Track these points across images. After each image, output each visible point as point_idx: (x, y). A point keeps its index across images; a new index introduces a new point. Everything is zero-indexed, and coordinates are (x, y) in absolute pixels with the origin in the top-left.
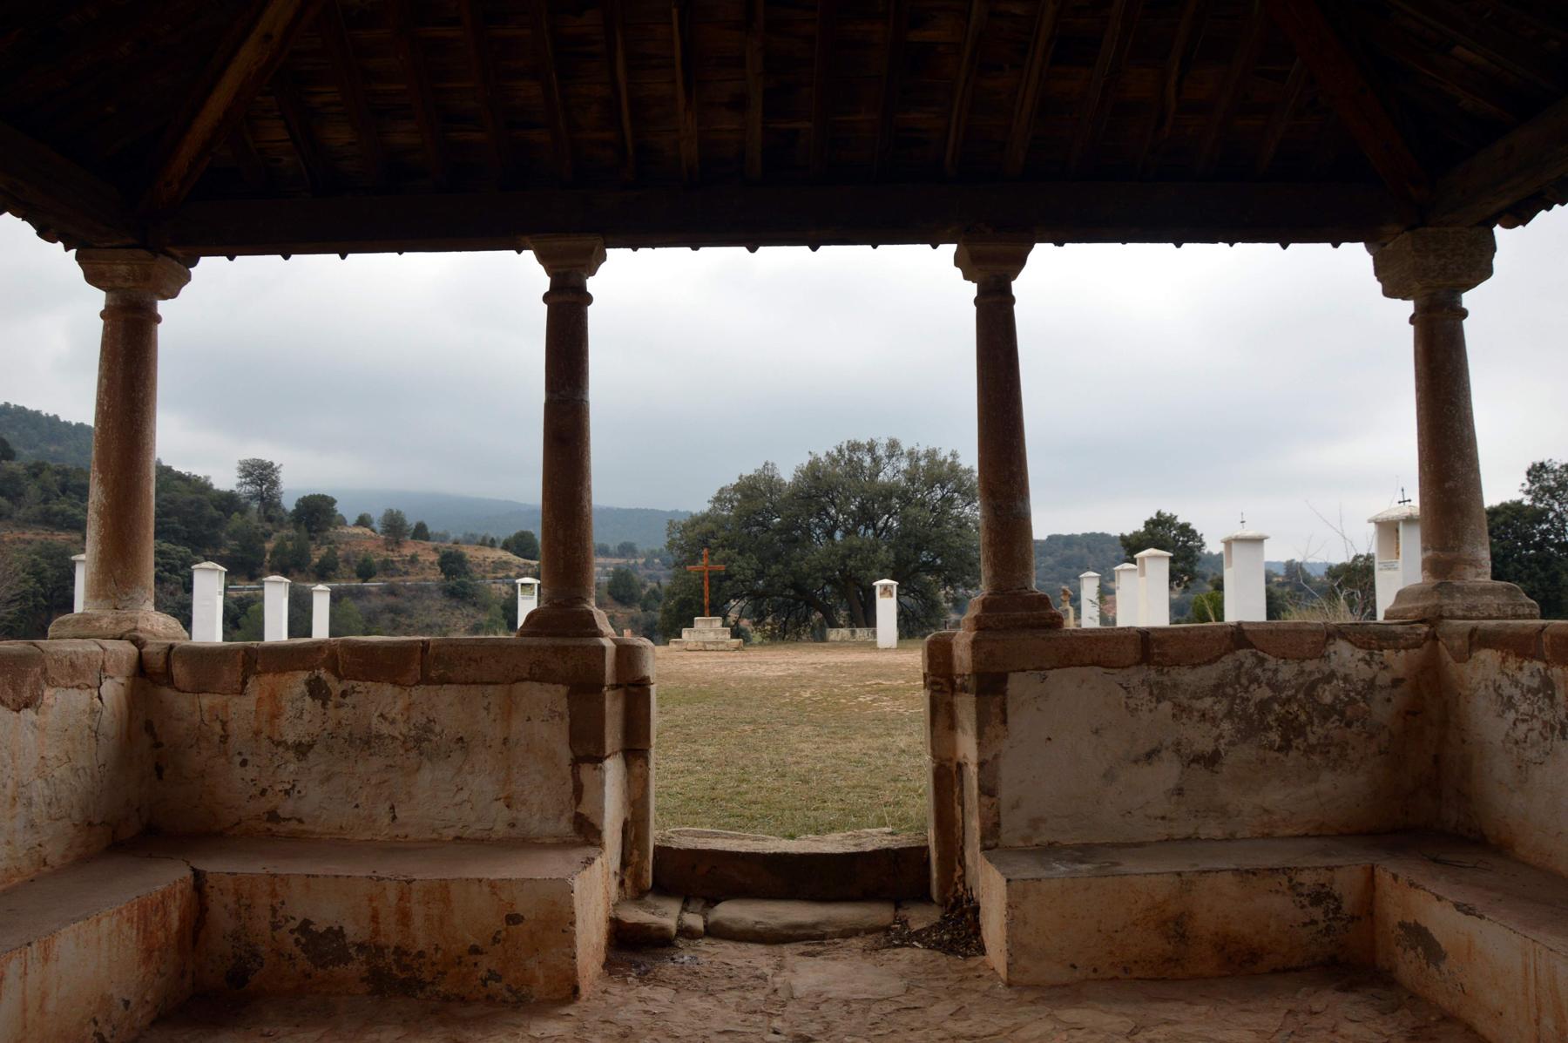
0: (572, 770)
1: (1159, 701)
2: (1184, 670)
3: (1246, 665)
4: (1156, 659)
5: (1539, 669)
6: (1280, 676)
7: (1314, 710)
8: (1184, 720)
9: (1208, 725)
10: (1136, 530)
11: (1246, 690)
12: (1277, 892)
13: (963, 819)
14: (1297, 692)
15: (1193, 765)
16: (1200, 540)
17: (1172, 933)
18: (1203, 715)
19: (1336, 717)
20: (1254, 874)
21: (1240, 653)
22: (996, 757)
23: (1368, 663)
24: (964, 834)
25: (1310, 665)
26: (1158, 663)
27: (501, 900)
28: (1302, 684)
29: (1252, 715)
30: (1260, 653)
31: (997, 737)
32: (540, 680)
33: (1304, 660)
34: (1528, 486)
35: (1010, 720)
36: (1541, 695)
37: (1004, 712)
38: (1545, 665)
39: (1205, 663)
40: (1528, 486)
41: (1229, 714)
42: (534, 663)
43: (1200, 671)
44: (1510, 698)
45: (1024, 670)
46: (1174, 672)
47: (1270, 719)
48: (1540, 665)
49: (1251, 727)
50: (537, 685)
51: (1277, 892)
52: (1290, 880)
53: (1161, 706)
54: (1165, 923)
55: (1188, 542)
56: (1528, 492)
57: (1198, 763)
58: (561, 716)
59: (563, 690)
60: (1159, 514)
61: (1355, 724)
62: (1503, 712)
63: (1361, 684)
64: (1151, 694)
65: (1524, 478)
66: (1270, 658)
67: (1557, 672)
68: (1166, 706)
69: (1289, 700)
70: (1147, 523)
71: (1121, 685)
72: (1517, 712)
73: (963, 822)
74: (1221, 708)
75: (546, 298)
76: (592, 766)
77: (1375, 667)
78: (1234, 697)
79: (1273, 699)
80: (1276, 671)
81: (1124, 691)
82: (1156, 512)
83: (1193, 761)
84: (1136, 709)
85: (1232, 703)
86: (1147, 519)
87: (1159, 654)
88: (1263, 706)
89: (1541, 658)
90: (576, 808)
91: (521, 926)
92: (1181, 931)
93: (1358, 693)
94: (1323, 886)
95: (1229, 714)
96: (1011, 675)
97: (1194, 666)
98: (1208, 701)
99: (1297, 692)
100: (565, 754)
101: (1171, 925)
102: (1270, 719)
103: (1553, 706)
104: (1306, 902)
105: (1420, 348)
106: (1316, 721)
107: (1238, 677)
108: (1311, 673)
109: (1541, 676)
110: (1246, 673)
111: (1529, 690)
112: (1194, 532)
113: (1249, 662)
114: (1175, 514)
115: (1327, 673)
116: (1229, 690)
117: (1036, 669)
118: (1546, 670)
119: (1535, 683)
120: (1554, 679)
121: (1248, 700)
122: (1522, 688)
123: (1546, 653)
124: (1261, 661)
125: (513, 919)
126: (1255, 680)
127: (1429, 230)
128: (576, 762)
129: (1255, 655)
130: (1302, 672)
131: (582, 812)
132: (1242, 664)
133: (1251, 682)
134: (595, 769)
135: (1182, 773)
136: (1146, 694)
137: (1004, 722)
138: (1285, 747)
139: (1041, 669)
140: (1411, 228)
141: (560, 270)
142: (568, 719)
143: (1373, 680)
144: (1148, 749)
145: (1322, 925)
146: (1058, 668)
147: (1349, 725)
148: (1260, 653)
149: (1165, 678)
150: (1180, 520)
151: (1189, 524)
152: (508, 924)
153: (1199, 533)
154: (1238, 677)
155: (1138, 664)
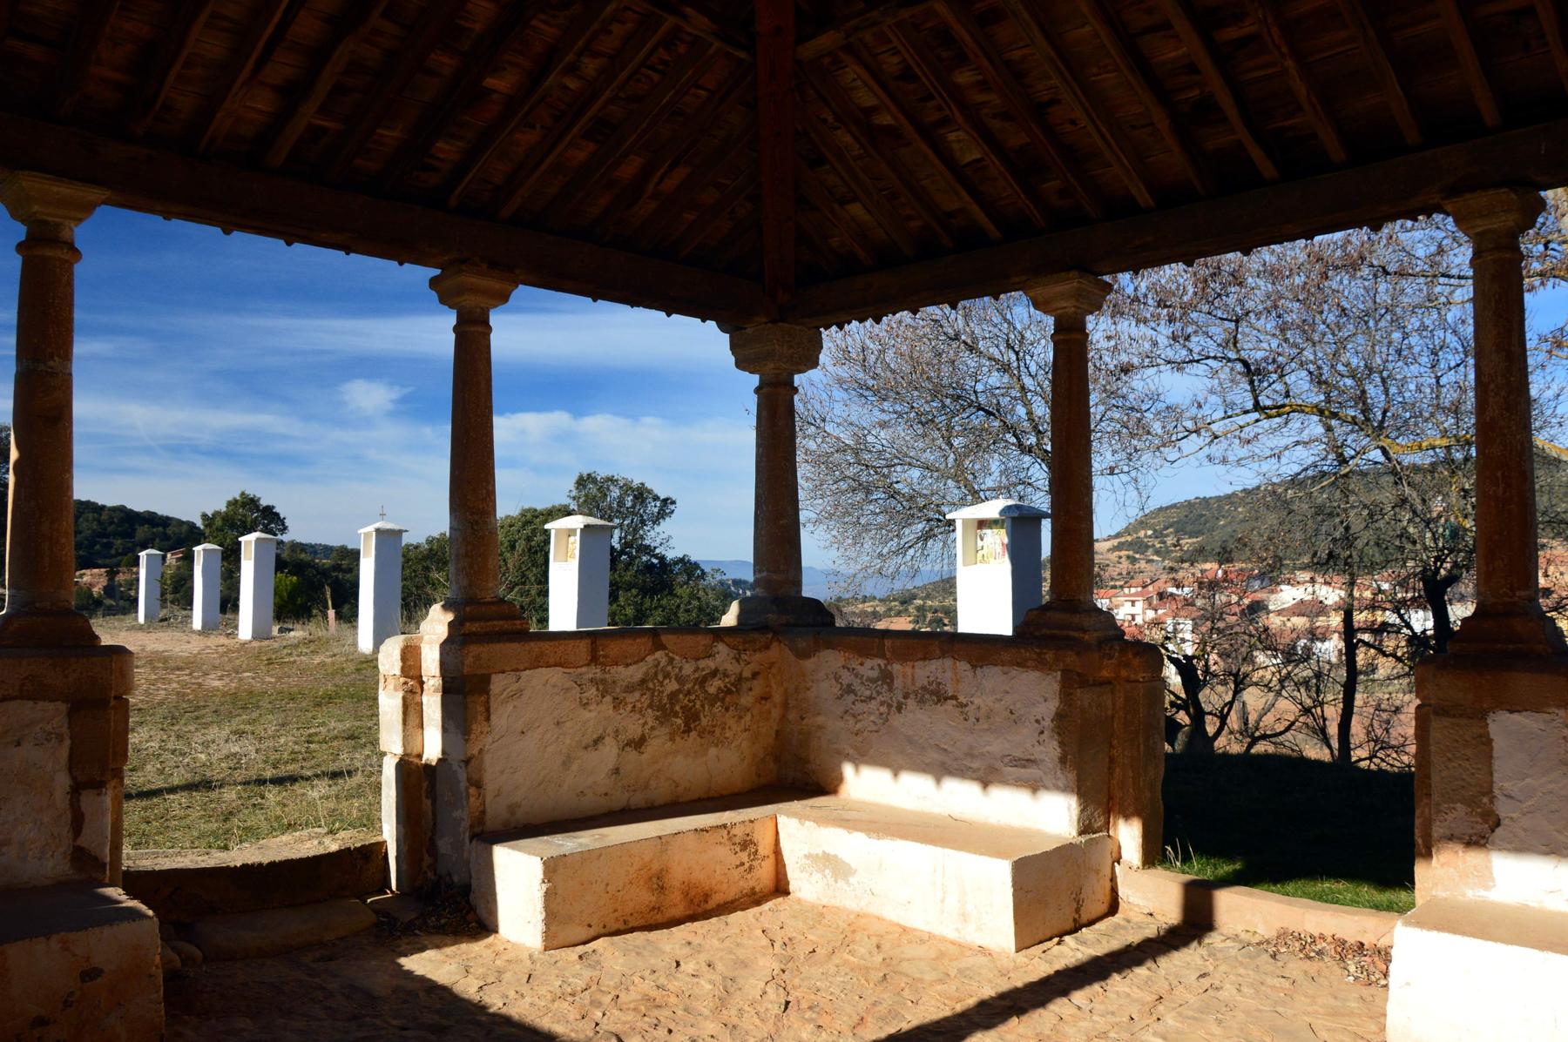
0: (71, 800)
1: (603, 697)
2: (621, 669)
3: (662, 665)
4: (601, 660)
5: (879, 665)
6: (683, 672)
7: (706, 699)
8: (622, 711)
9: (638, 716)
10: (218, 509)
11: (661, 684)
12: (721, 843)
13: (434, 814)
14: (695, 685)
15: (627, 749)
16: (283, 524)
17: (656, 886)
18: (634, 706)
19: (719, 704)
20: (707, 831)
21: (658, 654)
22: (481, 751)
23: (738, 661)
24: (435, 824)
25: (702, 663)
26: (601, 663)
27: (75, 955)
28: (697, 679)
29: (665, 704)
30: (671, 655)
31: (482, 733)
32: (33, 697)
33: (698, 659)
34: (574, 493)
35: (493, 717)
36: (880, 683)
37: (488, 710)
38: (885, 662)
39: (635, 663)
40: (574, 493)
41: (650, 706)
42: (26, 678)
43: (631, 668)
44: (849, 686)
45: (503, 672)
46: (614, 670)
47: (677, 708)
48: (882, 662)
49: (665, 715)
50: (31, 703)
51: (721, 843)
52: (729, 833)
53: (604, 699)
54: (651, 878)
55: (268, 524)
56: (574, 498)
57: (630, 746)
58: (60, 738)
59: (63, 707)
60: (243, 494)
61: (731, 708)
62: (842, 696)
63: (734, 677)
64: (598, 689)
65: (572, 486)
66: (677, 658)
67: (896, 668)
68: (608, 699)
69: (689, 693)
70: (229, 504)
71: (576, 682)
72: (856, 695)
73: (434, 814)
74: (646, 700)
75: (20, 247)
76: (95, 792)
77: (742, 664)
78: (654, 690)
79: (679, 691)
80: (681, 669)
81: (578, 689)
82: (240, 492)
83: (627, 745)
84: (587, 704)
85: (653, 696)
86: (230, 499)
87: (605, 656)
88: (673, 696)
89: (883, 656)
90: (75, 840)
91: (99, 980)
92: (661, 884)
93: (732, 684)
94: (748, 835)
95: (650, 706)
96: (494, 676)
97: (627, 665)
98: (637, 695)
99: (695, 685)
100: (63, 782)
101: (654, 880)
102: (677, 708)
103: (890, 690)
104: (738, 849)
105: (764, 414)
106: (707, 707)
107: (656, 674)
108: (703, 669)
109: (881, 669)
110: (662, 670)
111: (869, 679)
112: (277, 515)
113: (664, 662)
114: (258, 496)
115: (713, 668)
116: (651, 685)
117: (512, 671)
118: (886, 666)
119: (875, 674)
120: (894, 672)
121: (663, 692)
122: (861, 679)
123: (887, 653)
124: (671, 660)
125: (90, 974)
126: (667, 676)
127: (786, 325)
128: (76, 790)
129: (667, 655)
130: (697, 669)
131: (83, 845)
132: (659, 663)
133: (665, 678)
134: (99, 794)
135: (619, 755)
136: (594, 689)
137: (488, 719)
138: (688, 731)
139: (517, 670)
140: (774, 321)
141: (50, 219)
142: (67, 742)
143: (741, 674)
144: (595, 736)
145: (747, 865)
146: (530, 669)
147: (727, 709)
148: (671, 655)
149: (607, 676)
150: (264, 503)
151: (273, 507)
152: (83, 981)
153: (282, 516)
154: (656, 674)
155: (588, 665)
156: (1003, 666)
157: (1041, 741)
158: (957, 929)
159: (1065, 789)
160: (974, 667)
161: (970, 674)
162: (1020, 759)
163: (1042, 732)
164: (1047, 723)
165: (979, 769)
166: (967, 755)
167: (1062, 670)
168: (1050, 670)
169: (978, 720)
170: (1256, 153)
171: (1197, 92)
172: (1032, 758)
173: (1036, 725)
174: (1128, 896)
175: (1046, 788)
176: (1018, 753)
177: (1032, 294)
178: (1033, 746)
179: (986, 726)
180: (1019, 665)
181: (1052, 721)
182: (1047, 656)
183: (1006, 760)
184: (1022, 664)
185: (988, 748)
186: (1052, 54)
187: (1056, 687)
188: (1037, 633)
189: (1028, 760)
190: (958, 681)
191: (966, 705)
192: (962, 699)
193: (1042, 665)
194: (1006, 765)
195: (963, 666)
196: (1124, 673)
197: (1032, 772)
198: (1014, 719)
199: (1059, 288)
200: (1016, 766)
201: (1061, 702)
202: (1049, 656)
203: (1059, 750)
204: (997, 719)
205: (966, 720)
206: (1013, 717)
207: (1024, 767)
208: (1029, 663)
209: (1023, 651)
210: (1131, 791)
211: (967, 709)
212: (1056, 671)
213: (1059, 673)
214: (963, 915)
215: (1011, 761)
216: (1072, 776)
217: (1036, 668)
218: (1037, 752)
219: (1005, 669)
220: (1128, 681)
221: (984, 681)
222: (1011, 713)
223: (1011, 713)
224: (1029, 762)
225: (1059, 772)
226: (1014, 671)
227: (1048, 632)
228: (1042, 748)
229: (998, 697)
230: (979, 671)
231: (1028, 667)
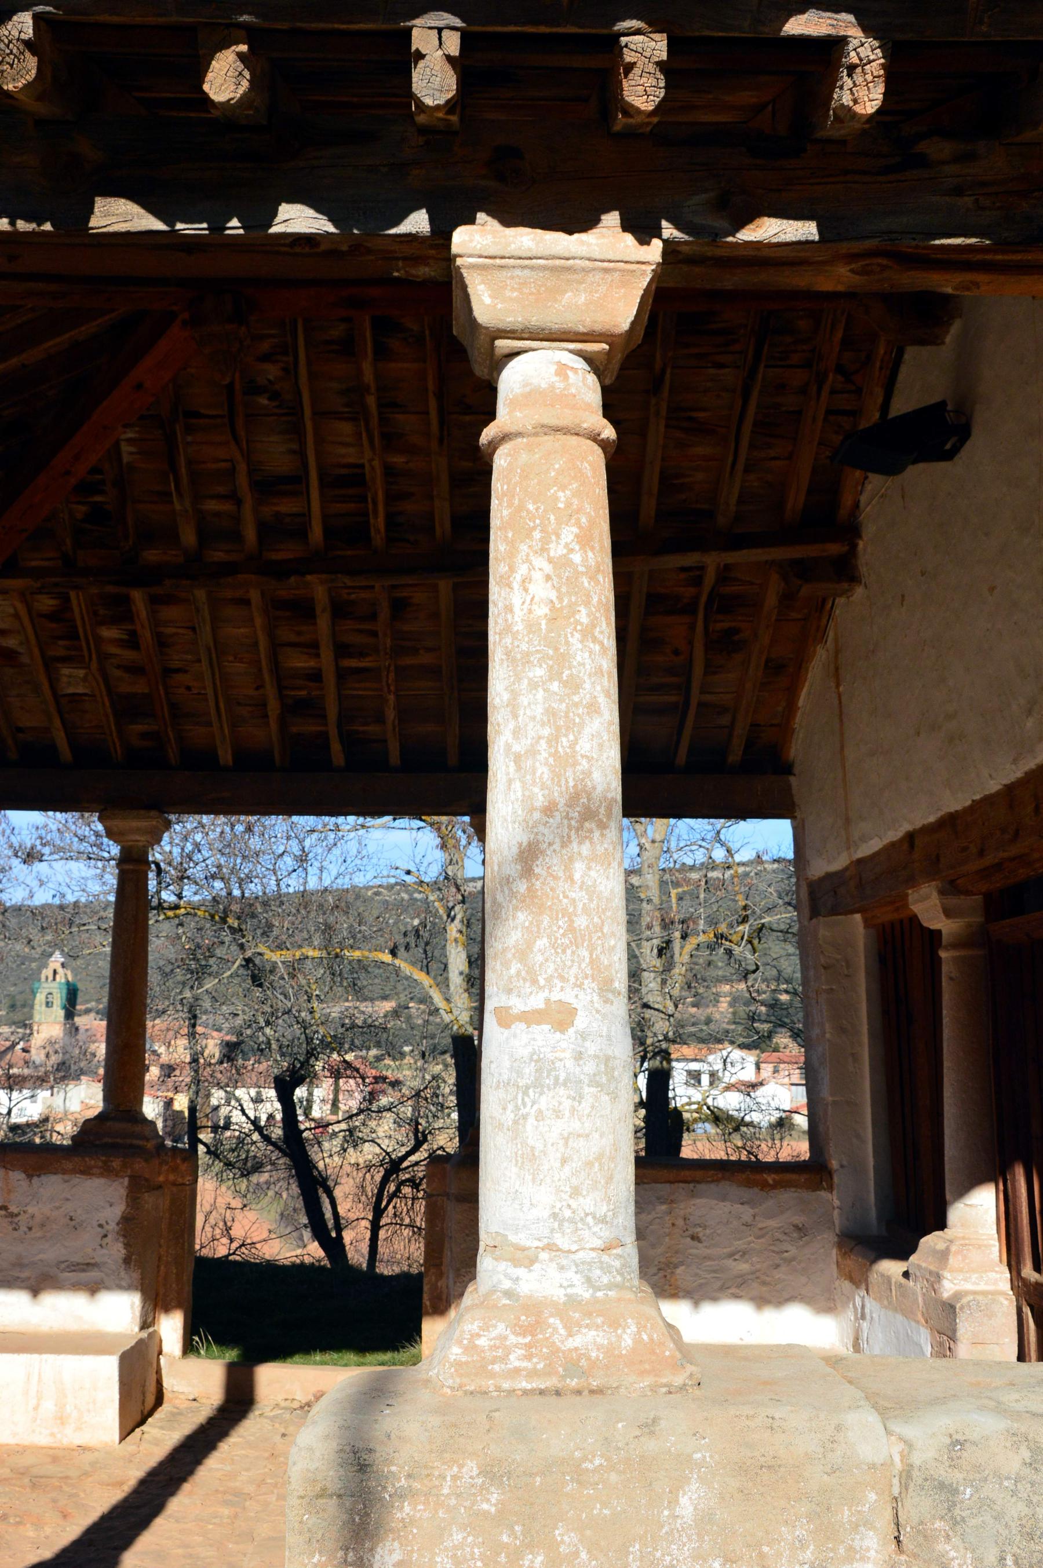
156: (64, 1174)
157: (104, 1245)
158: (53, 1435)
159: (129, 1288)
160: (30, 1177)
161: (25, 1183)
162: (78, 1264)
163: (105, 1236)
164: (112, 1226)
165: (29, 1278)
166: (14, 1265)
167: (130, 1177)
168: (116, 1176)
169: (30, 1229)
170: (336, 747)
171: (304, 693)
172: (92, 1261)
173: (100, 1229)
174: (173, 1385)
175: (108, 1288)
176: (76, 1258)
177: (108, 824)
178: (94, 1250)
179: (39, 1234)
180: (82, 1173)
181: (118, 1224)
182: (114, 1164)
183: (63, 1266)
184: (86, 1172)
185: (41, 1256)
186: (212, 644)
187: (123, 1192)
188: (97, 1142)
189: (88, 1264)
190: (9, 1191)
191: (17, 1215)
192: (13, 1209)
193: (108, 1172)
194: (63, 1271)
195: (17, 1176)
196: (172, 1177)
197: (94, 1275)
198: (74, 1224)
199: (135, 824)
200: (74, 1271)
201: (128, 1206)
202: (116, 1164)
203: (124, 1251)
204: (54, 1226)
205: (15, 1229)
206: (73, 1223)
207: (84, 1271)
208: (95, 1170)
209: (87, 1159)
210: (174, 1285)
211: (19, 1218)
212: (123, 1177)
213: (126, 1180)
214: (61, 1418)
215: (68, 1267)
216: (136, 1275)
217: (101, 1175)
218: (101, 1255)
219: (66, 1177)
220: (174, 1184)
221: (41, 1190)
222: (71, 1219)
223: (71, 1219)
224: (88, 1266)
225: (123, 1273)
226: (77, 1179)
227: (110, 1141)
228: (105, 1251)
229: (57, 1204)
230: (35, 1180)
231: (93, 1174)
